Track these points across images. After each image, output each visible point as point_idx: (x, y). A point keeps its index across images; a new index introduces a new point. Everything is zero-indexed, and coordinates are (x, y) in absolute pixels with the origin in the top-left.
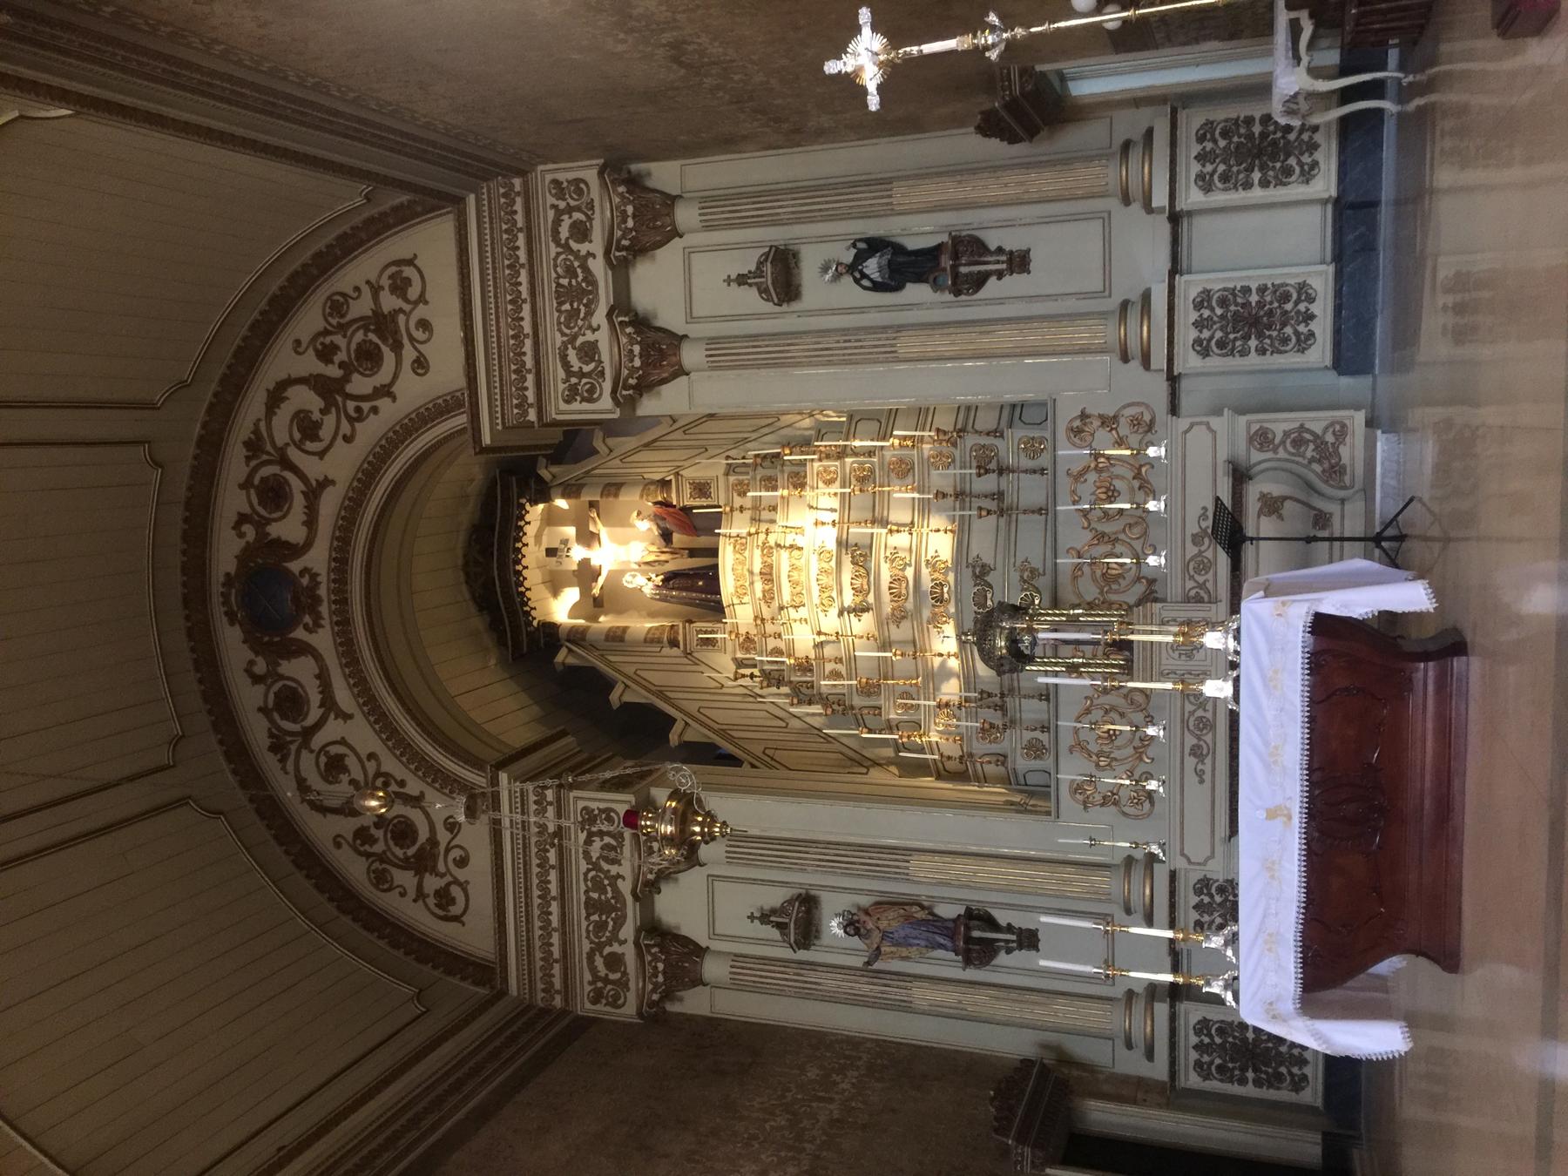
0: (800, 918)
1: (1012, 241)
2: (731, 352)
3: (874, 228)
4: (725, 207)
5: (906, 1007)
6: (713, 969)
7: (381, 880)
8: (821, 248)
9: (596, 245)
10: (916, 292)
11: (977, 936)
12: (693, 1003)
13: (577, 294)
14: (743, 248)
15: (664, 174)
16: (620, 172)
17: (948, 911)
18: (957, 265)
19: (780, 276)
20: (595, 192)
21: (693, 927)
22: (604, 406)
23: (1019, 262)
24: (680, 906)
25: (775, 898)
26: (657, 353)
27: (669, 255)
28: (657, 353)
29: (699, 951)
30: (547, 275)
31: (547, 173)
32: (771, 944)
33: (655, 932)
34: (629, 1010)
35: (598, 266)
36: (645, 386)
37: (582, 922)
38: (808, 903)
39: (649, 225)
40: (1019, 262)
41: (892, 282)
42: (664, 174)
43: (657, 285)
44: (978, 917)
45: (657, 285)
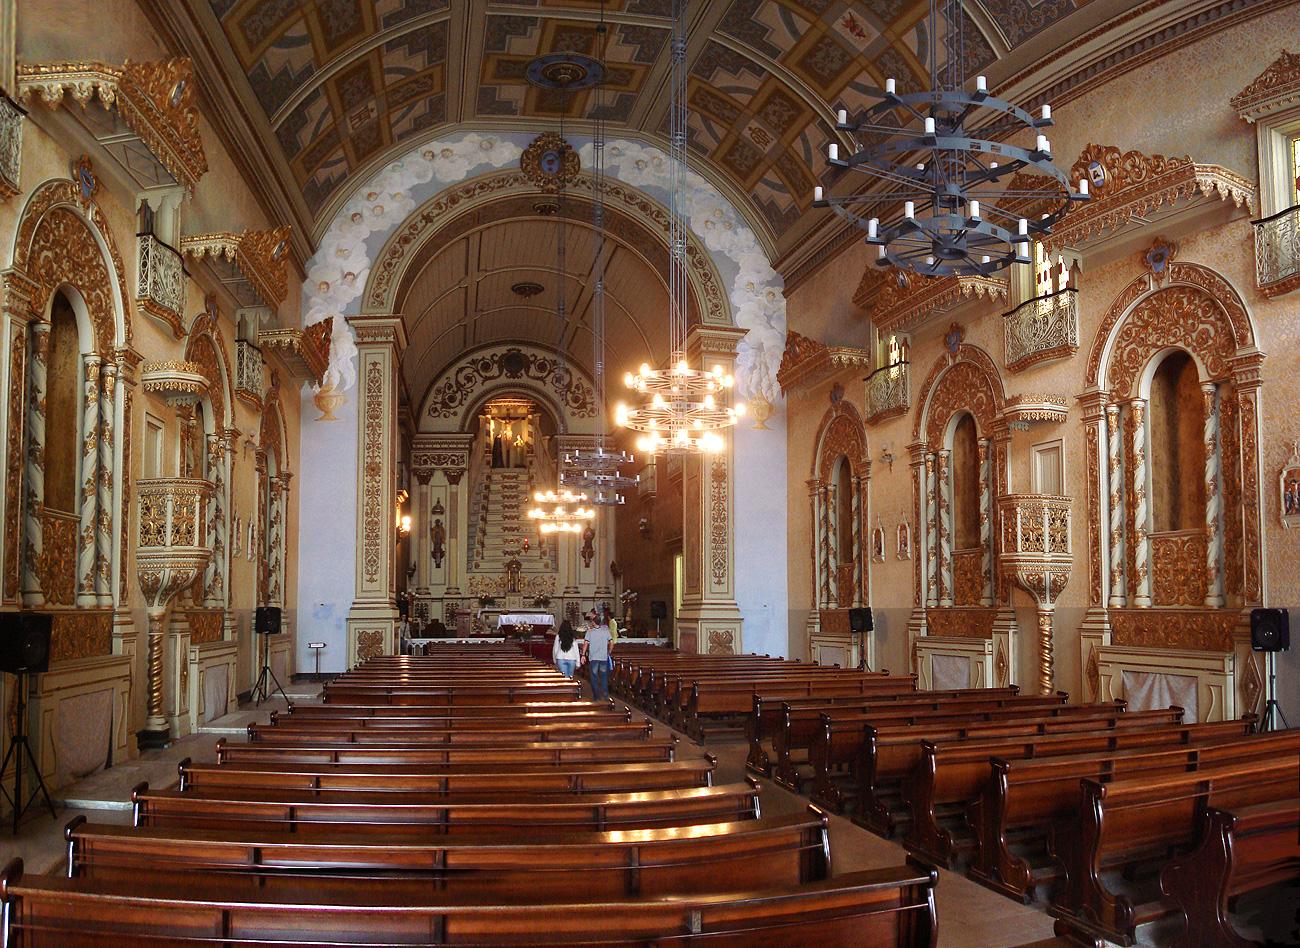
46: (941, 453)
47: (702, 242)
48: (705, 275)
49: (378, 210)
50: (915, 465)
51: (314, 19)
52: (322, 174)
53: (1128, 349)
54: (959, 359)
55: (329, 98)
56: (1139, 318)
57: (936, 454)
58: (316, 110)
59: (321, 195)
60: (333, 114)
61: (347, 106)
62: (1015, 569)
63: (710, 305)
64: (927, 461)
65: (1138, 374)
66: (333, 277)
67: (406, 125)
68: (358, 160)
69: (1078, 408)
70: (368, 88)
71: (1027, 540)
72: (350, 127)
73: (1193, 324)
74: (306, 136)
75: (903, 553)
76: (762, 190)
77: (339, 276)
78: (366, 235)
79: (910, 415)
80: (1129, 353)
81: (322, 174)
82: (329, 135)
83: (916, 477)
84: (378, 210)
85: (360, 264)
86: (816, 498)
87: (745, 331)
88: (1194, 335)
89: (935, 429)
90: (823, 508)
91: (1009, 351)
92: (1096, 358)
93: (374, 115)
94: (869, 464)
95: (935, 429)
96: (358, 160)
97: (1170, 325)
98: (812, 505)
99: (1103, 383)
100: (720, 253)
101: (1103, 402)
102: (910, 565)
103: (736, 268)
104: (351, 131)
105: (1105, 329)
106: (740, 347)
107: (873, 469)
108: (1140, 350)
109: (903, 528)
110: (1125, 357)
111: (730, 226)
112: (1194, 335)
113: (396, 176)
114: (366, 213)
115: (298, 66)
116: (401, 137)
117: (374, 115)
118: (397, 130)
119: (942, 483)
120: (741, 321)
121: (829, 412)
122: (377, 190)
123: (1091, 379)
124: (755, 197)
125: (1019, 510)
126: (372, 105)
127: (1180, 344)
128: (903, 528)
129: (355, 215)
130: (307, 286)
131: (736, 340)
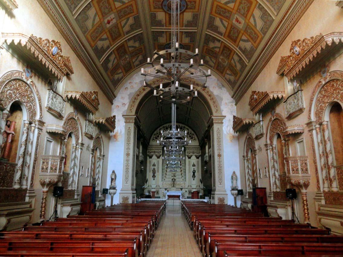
0: (154, 165)
1: (195, 179)
2: (189, 162)
3: (196, 172)
4: (198, 162)
5: (149, 172)
6: (150, 159)
7: (155, 135)
8: (196, 168)
9: (196, 154)
10: (193, 174)
11: (154, 176)
12: (148, 158)
13: (193, 153)
14: (196, 164)
15: (200, 158)
16: (200, 156)
17: (155, 175)
18: (194, 176)
19: (194, 165)
20: (199, 154)
21: (153, 158)
22: (187, 154)
23: (194, 180)
24: (154, 157)
25: (155, 163)
26: (189, 158)
27: (195, 158)
28: (189, 158)
29: (151, 158)
30: (195, 151)
31: (200, 151)
32: (152, 164)
33: (152, 156)
34: (148, 154)
35: (195, 154)
36: (188, 157)
37: (154, 151)
38: (155, 166)
39: (198, 158)
40: (194, 180)
41: (193, 172)
42: (200, 158)
43: (194, 157)
44: (155, 177)
45: (194, 157)
46: (273, 146)
47: (212, 93)
48: (214, 102)
49: (132, 87)
50: (267, 150)
51: (108, 34)
52: (116, 77)
53: (320, 105)
54: (275, 118)
55: (115, 54)
56: (322, 94)
57: (272, 146)
58: (112, 58)
59: (117, 83)
60: (117, 59)
61: (121, 57)
62: (290, 180)
63: (215, 110)
64: (270, 149)
65: (323, 113)
66: (120, 104)
67: (137, 63)
68: (126, 73)
69: (307, 127)
70: (125, 52)
71: (293, 170)
72: (122, 63)
73: (339, 92)
74: (110, 65)
75: (266, 175)
76: (228, 77)
77: (121, 104)
78: (129, 93)
79: (265, 135)
80: (320, 107)
81: (116, 77)
82: (117, 65)
83: (267, 153)
84: (132, 87)
85: (127, 101)
86: (245, 161)
87: (225, 116)
88: (339, 95)
89: (271, 139)
90: (247, 163)
91: (286, 113)
92: (310, 111)
93: (128, 59)
94: (256, 150)
95: (271, 139)
96: (126, 73)
97: (331, 94)
98: (244, 162)
99: (313, 118)
100: (217, 96)
101: (314, 124)
102: (268, 179)
103: (222, 99)
104: (122, 64)
105: (311, 100)
106: (224, 121)
107: (257, 151)
108: (323, 105)
109: (265, 168)
110: (319, 109)
111: (220, 88)
112: (339, 95)
113: (137, 78)
114: (129, 88)
115: (105, 46)
116: (137, 66)
117: (128, 59)
118: (135, 64)
119: (274, 154)
120: (224, 114)
121: (247, 136)
122: (132, 82)
123: (309, 118)
124: (225, 78)
125: (290, 161)
126: (127, 57)
127: (335, 100)
128: (265, 168)
129: (126, 88)
130: (113, 106)
131: (223, 119)
